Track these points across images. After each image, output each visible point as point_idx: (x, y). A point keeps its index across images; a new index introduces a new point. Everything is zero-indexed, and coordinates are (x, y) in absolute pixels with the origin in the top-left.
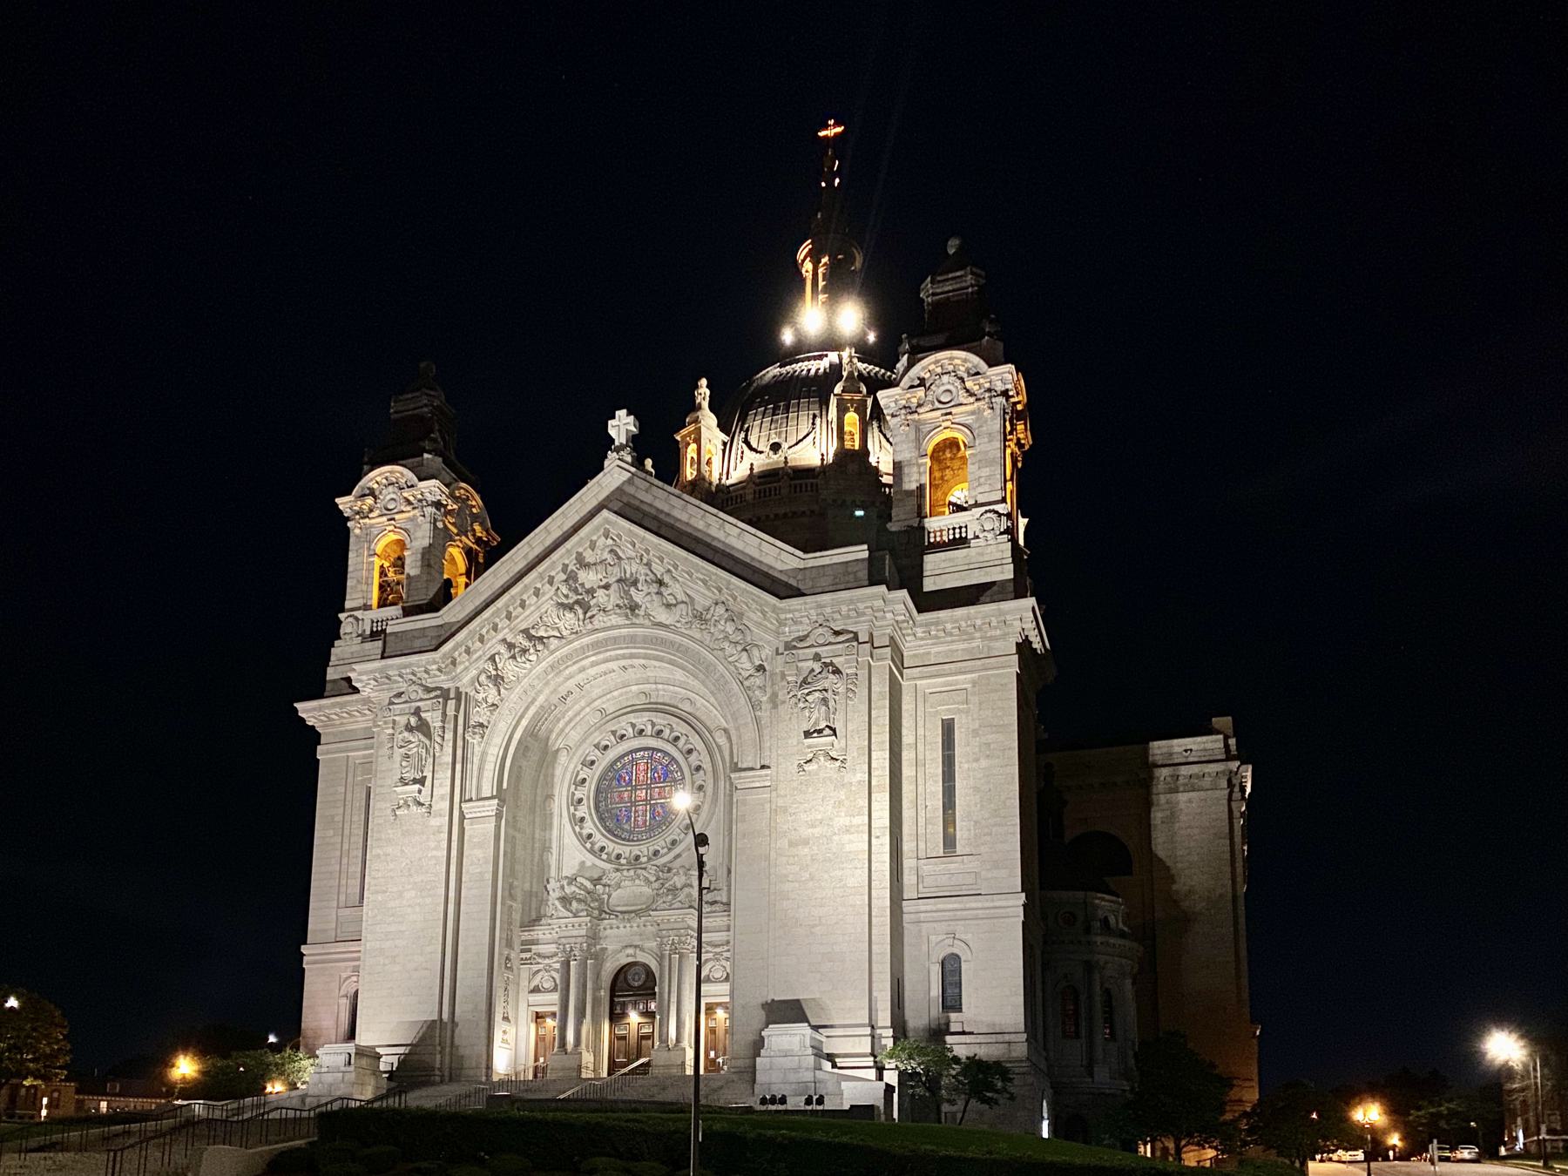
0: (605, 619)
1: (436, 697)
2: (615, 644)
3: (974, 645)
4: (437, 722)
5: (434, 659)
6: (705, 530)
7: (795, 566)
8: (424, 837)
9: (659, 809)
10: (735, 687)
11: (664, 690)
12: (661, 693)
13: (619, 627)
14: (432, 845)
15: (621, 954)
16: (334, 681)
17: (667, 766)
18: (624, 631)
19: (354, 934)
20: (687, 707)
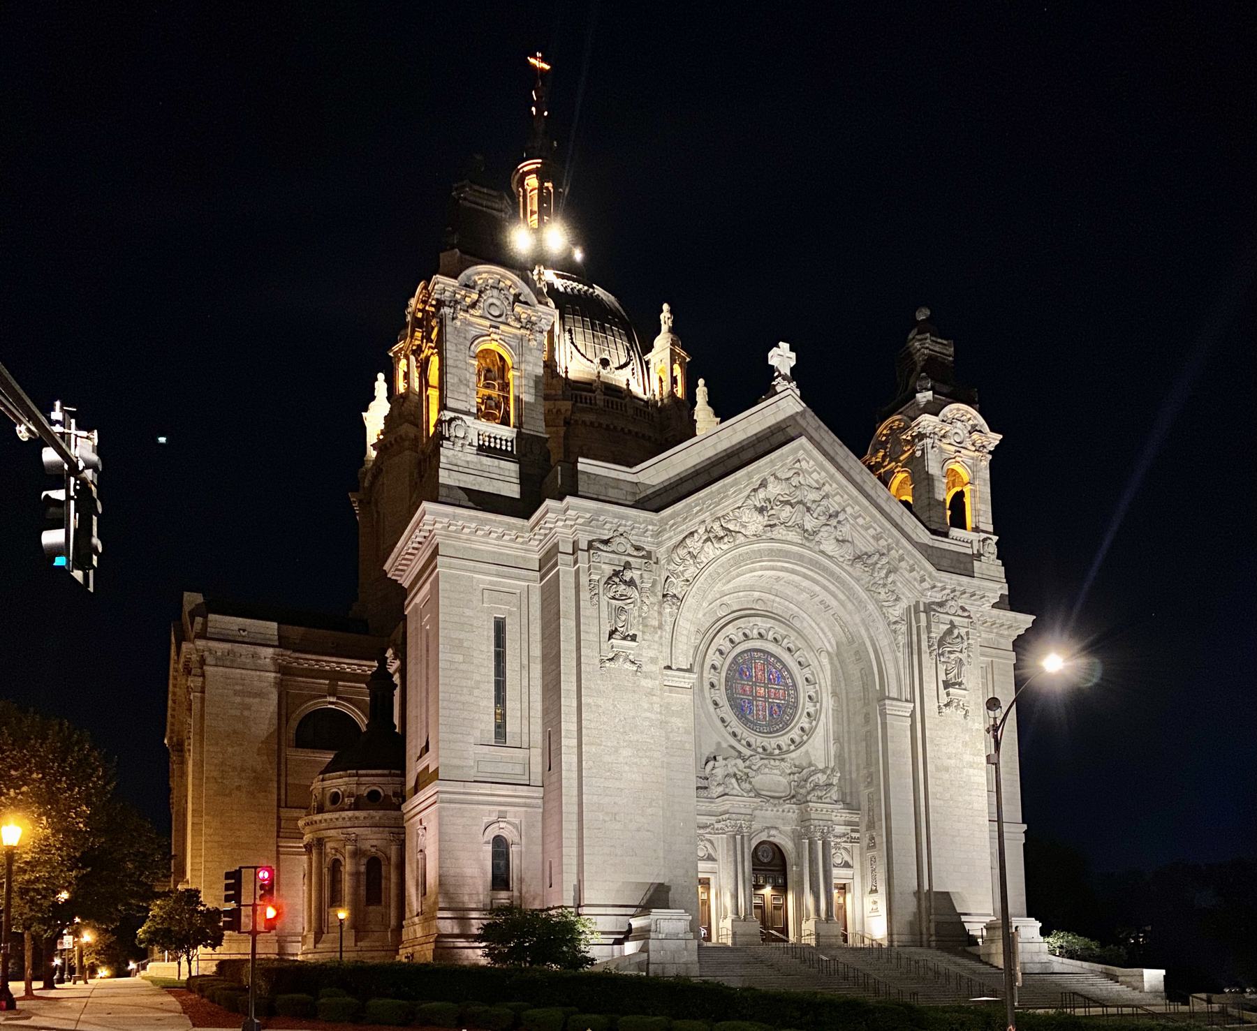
0: (785, 532)
1: (643, 557)
2: (786, 557)
3: (990, 637)
5: (652, 519)
6: (862, 484)
7: (926, 542)
8: (636, 696)
9: (775, 708)
10: (881, 626)
12: (775, 605)
14: (646, 706)
15: (763, 833)
17: (780, 671)
18: (795, 549)
19: (505, 776)
20: (797, 623)
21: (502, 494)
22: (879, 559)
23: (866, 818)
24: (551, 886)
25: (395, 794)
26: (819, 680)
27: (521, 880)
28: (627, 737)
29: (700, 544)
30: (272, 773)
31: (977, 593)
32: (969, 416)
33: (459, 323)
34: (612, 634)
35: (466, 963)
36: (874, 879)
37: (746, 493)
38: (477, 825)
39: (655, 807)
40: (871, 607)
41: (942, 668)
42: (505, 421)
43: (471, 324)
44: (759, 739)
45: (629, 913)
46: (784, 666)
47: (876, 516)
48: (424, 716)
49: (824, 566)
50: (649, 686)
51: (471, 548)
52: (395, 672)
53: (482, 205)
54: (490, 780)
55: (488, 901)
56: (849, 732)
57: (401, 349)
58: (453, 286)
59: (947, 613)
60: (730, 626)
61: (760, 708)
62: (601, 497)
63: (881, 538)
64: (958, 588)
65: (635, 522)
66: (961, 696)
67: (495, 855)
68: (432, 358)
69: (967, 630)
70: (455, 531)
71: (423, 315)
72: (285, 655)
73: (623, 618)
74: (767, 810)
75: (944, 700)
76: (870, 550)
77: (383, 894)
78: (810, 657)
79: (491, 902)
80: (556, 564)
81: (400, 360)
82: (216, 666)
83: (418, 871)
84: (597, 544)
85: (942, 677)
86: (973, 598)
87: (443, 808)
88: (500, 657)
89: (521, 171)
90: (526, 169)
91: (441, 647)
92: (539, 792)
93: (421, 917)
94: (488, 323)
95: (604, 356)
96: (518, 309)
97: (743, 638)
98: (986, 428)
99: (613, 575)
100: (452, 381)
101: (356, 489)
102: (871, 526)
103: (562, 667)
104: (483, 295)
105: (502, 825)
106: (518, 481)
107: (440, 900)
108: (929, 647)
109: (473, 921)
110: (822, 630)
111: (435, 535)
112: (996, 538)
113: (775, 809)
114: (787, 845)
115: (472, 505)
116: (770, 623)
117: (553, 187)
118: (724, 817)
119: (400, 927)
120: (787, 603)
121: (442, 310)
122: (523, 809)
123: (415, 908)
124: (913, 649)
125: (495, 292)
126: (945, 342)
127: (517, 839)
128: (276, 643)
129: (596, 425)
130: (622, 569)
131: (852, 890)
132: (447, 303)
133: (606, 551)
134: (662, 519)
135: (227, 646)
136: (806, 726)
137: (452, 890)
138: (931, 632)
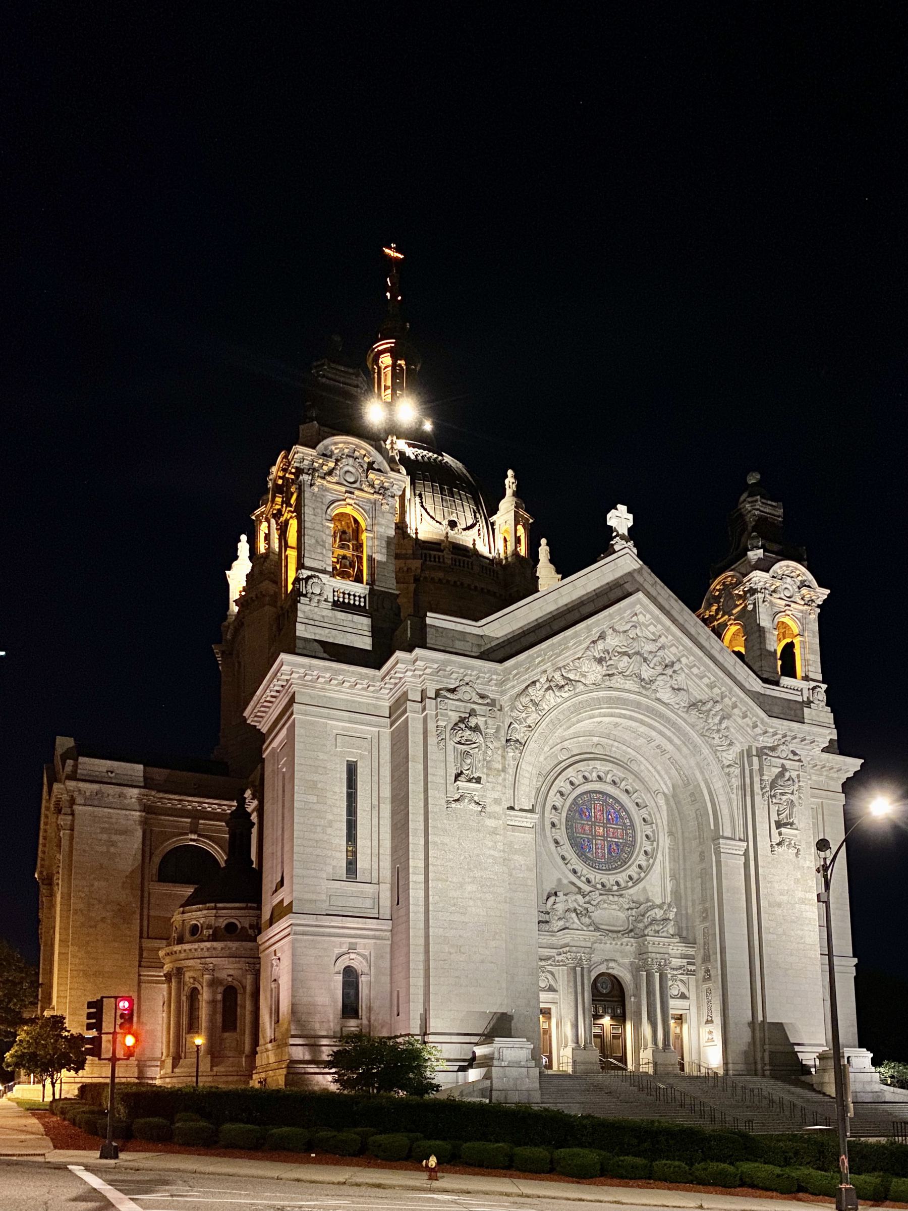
0: (622, 681)
1: (487, 705)
2: (624, 704)
3: (821, 779)
4: (492, 729)
5: (496, 669)
6: (696, 636)
7: (758, 690)
8: (481, 835)
9: (614, 846)
10: (715, 768)
11: (617, 748)
12: (614, 749)
13: (629, 691)
14: (490, 844)
16: (306, 640)
17: (618, 811)
18: (633, 696)
19: (356, 910)
20: (634, 767)
21: (355, 646)
22: (713, 707)
23: (702, 951)
24: (398, 1015)
25: (251, 926)
26: (656, 820)
27: (370, 1009)
28: (471, 874)
29: (541, 692)
30: (136, 905)
31: (807, 738)
32: (798, 572)
33: (316, 489)
34: (458, 776)
35: (316, 1088)
36: (710, 1009)
37: (585, 645)
38: (329, 956)
39: (498, 940)
40: (706, 751)
41: (774, 809)
42: (358, 579)
43: (327, 490)
44: (599, 876)
45: (472, 1041)
46: (622, 806)
47: (709, 666)
48: (279, 854)
49: (661, 713)
50: (494, 826)
51: (325, 696)
52: (253, 812)
53: (339, 382)
54: (341, 913)
55: (338, 1029)
56: (685, 869)
57: (262, 513)
58: (311, 455)
59: (779, 757)
60: (570, 769)
61: (600, 846)
62: (448, 649)
63: (715, 686)
64: (789, 733)
65: (481, 672)
66: (792, 835)
67: (346, 984)
68: (291, 521)
69: (798, 773)
70: (311, 681)
71: (283, 482)
72: (150, 795)
73: (468, 761)
74: (606, 943)
75: (776, 839)
76: (704, 697)
77: (238, 1022)
78: (647, 798)
79: (342, 1029)
80: (405, 711)
81: (261, 522)
82: (85, 805)
83: (271, 1000)
84: (444, 693)
85: (774, 817)
86: (803, 743)
87: (296, 940)
88: (352, 798)
89: (376, 350)
90: (380, 348)
91: (296, 787)
92: (387, 925)
93: (273, 1043)
94: (343, 489)
95: (452, 518)
96: (372, 476)
97: (582, 780)
98: (814, 583)
99: (459, 721)
100: (309, 542)
101: (219, 641)
102: (705, 676)
103: (410, 807)
104: (339, 463)
105: (352, 956)
106: (370, 634)
107: (293, 1027)
108: (762, 789)
109: (324, 1048)
110: (658, 773)
111: (291, 684)
112: (824, 686)
113: (614, 943)
114: (626, 977)
115: (328, 657)
116: (609, 766)
117: (406, 365)
118: (565, 950)
119: (254, 1053)
120: (624, 748)
121: (301, 477)
122: (374, 941)
123: (269, 1034)
124: (746, 790)
125: (351, 461)
126: (774, 504)
127: (366, 970)
128: (142, 784)
129: (444, 581)
130: (468, 715)
131: (688, 1021)
132: (305, 471)
133: (453, 699)
134: (506, 669)
135: (96, 787)
136: (644, 864)
137: (304, 1017)
138: (763, 775)
